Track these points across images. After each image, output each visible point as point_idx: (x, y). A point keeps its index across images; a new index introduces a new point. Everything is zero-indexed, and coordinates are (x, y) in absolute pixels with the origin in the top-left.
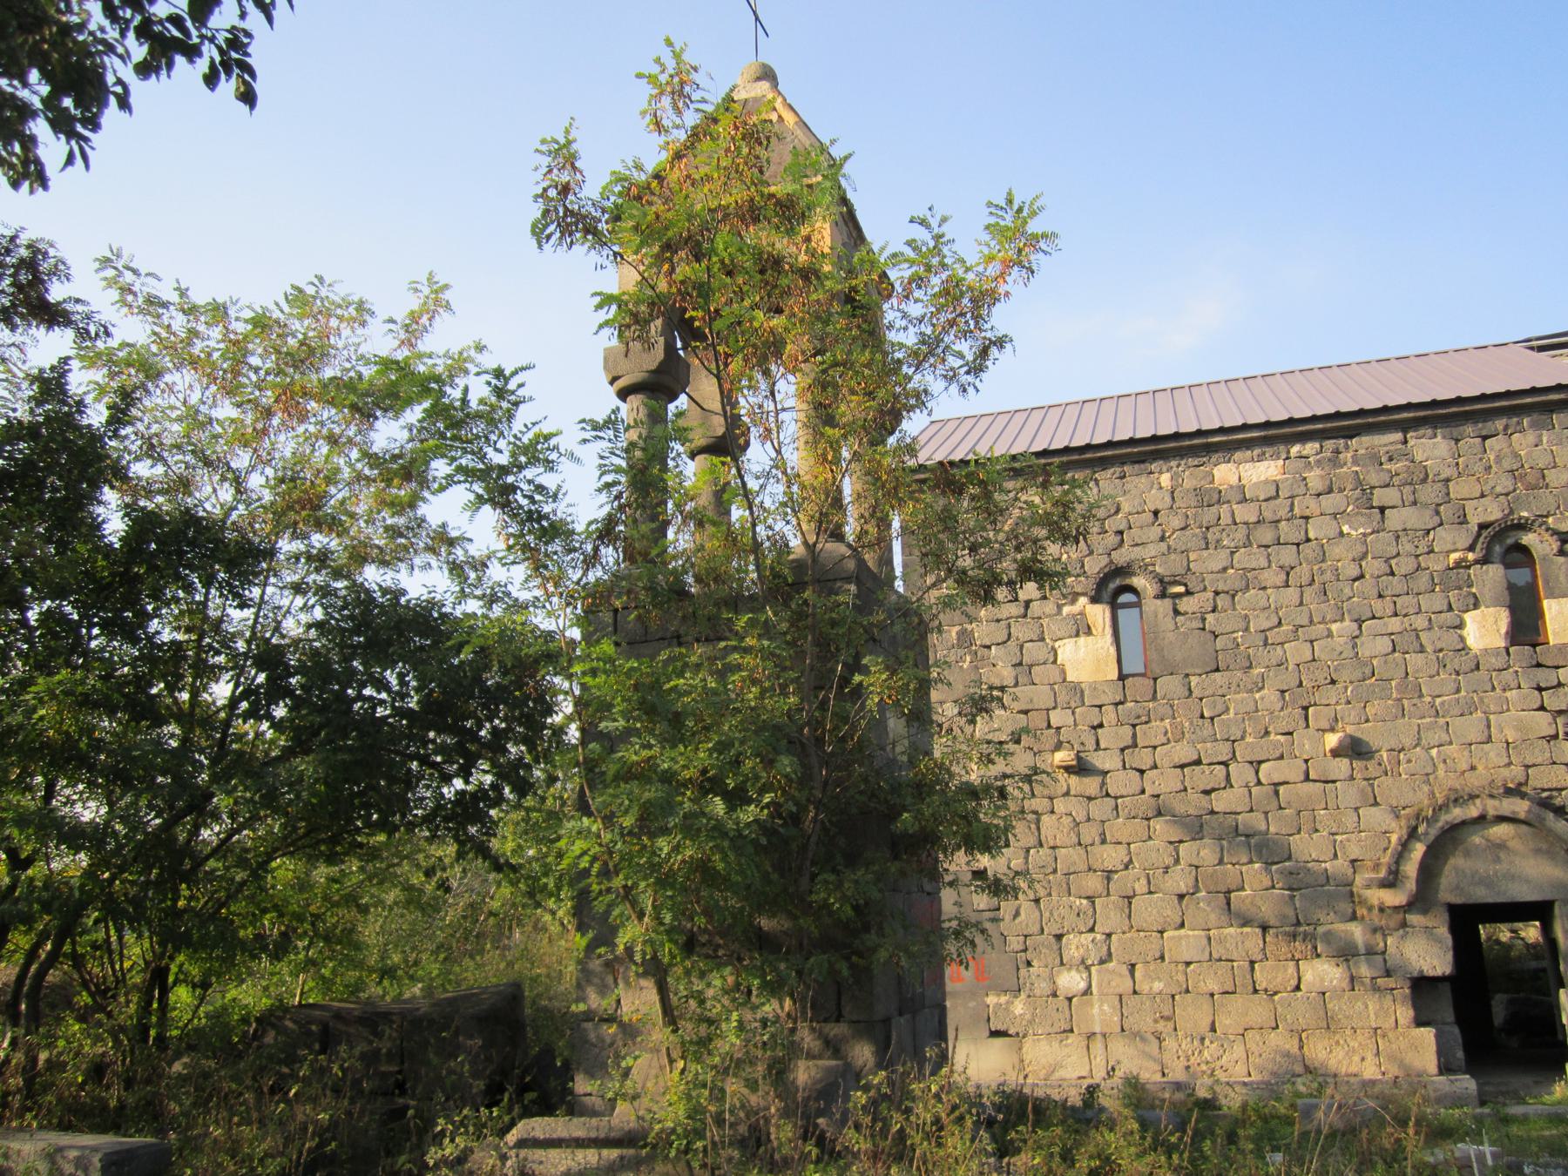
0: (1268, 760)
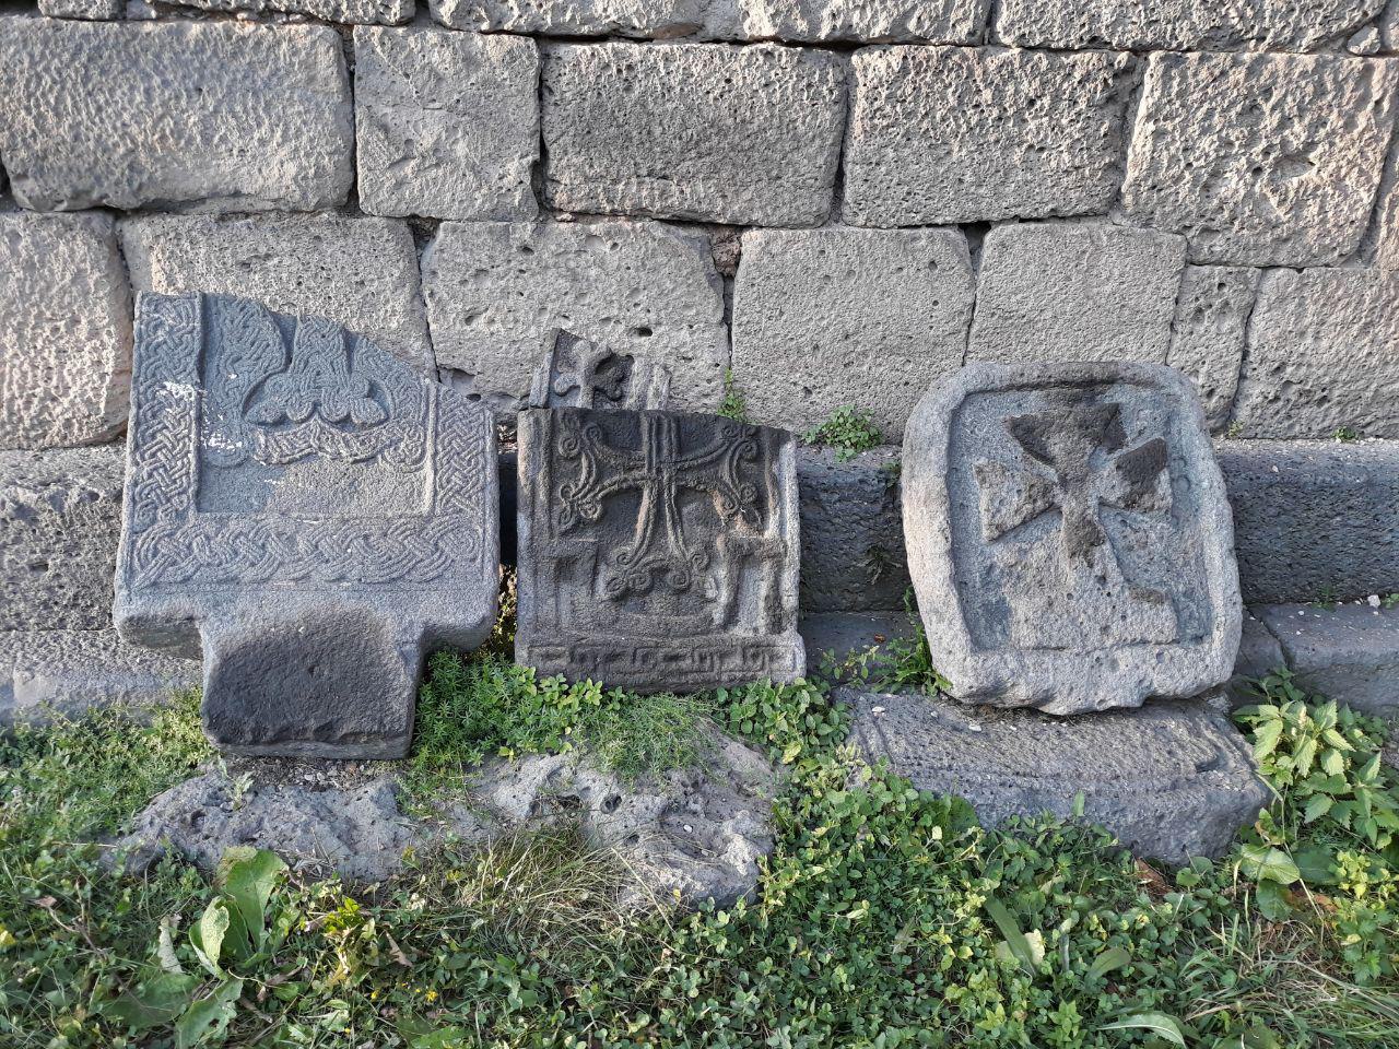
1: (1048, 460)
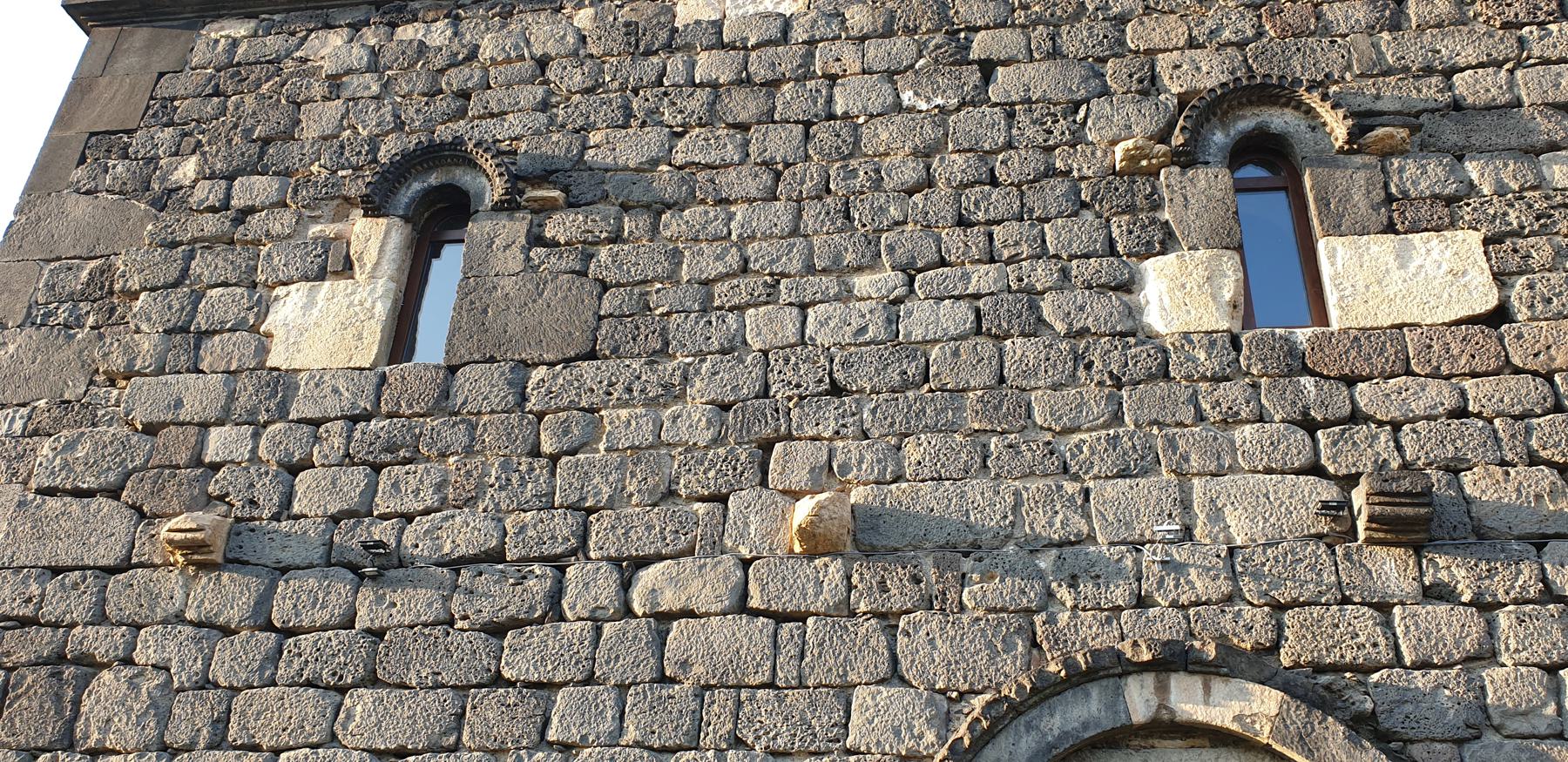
0: (660, 558)
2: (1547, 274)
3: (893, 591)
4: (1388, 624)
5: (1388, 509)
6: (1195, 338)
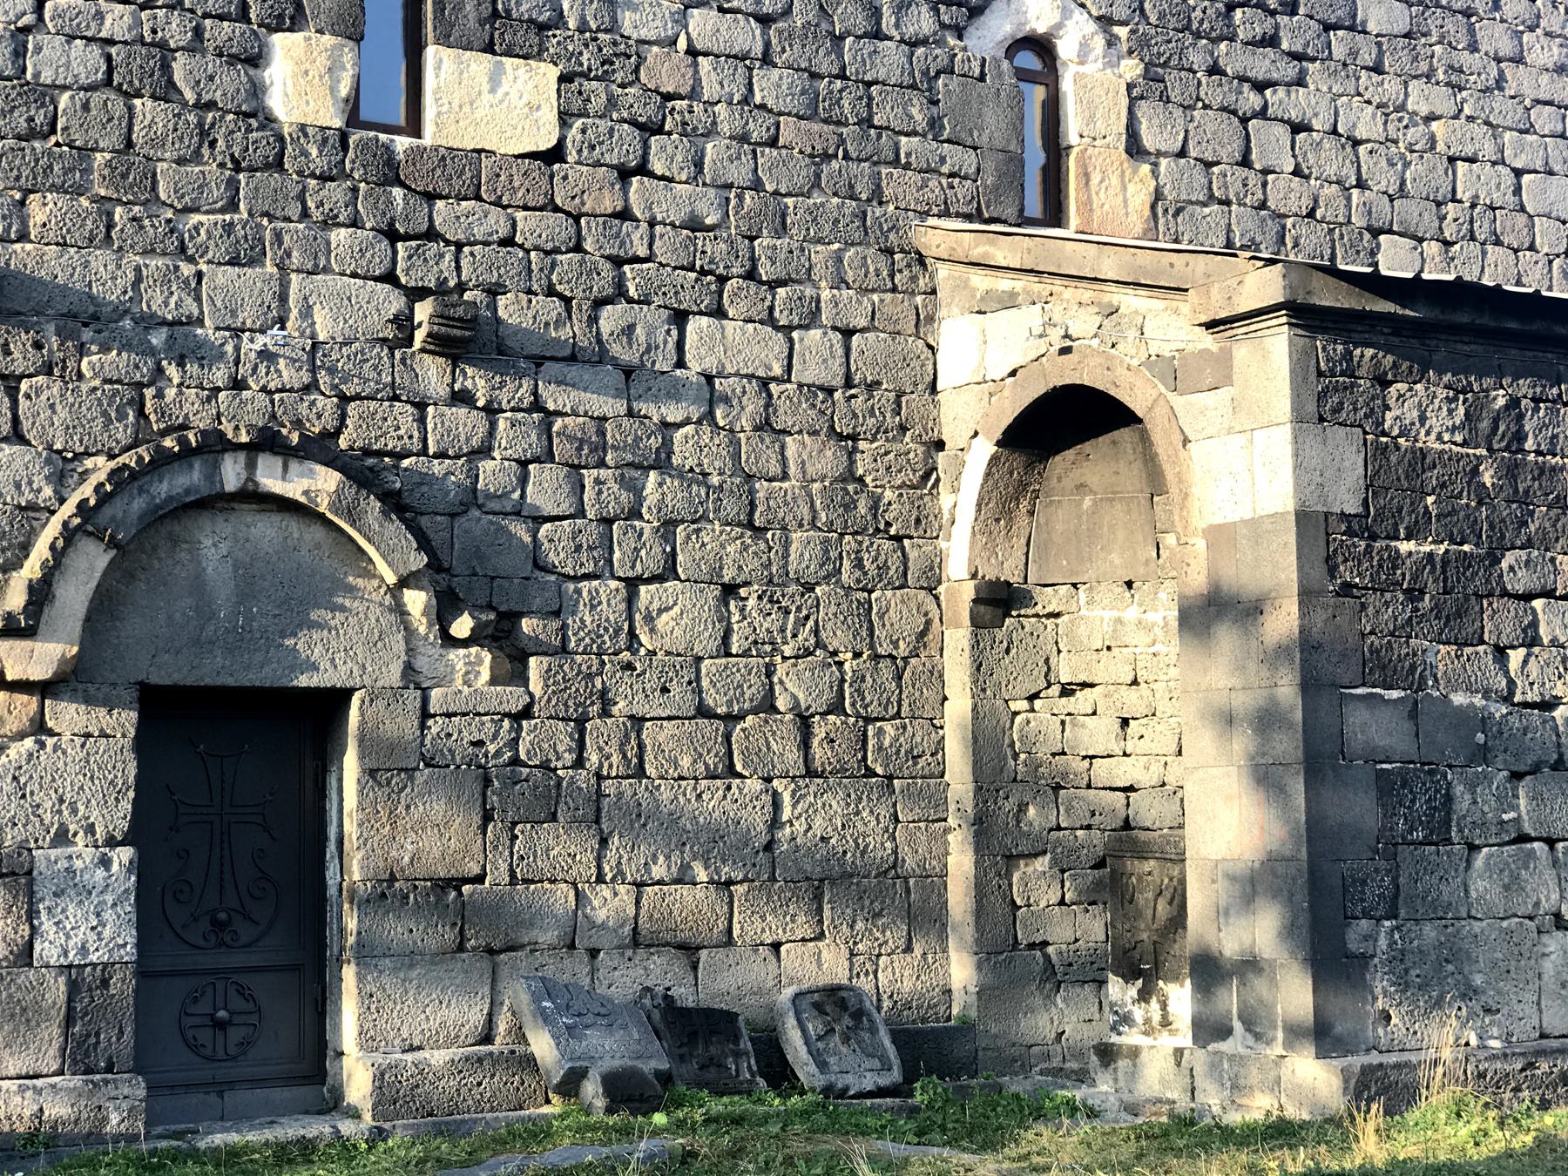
1: (827, 1014)
2: (597, 121)
3: (16, 355)
4: (422, 420)
5: (443, 329)
6: (310, 131)
